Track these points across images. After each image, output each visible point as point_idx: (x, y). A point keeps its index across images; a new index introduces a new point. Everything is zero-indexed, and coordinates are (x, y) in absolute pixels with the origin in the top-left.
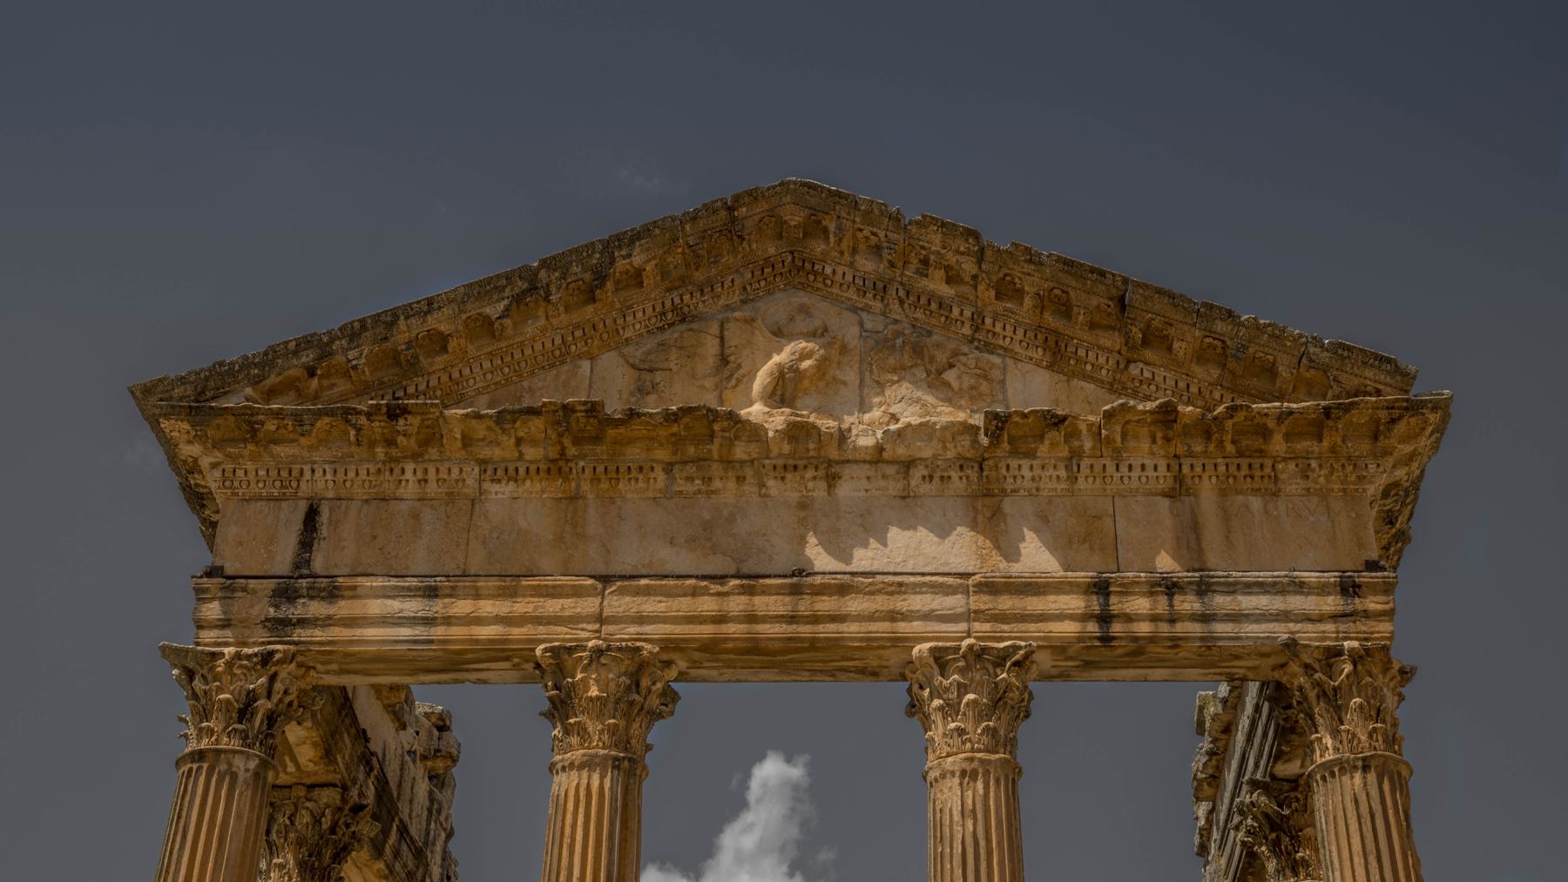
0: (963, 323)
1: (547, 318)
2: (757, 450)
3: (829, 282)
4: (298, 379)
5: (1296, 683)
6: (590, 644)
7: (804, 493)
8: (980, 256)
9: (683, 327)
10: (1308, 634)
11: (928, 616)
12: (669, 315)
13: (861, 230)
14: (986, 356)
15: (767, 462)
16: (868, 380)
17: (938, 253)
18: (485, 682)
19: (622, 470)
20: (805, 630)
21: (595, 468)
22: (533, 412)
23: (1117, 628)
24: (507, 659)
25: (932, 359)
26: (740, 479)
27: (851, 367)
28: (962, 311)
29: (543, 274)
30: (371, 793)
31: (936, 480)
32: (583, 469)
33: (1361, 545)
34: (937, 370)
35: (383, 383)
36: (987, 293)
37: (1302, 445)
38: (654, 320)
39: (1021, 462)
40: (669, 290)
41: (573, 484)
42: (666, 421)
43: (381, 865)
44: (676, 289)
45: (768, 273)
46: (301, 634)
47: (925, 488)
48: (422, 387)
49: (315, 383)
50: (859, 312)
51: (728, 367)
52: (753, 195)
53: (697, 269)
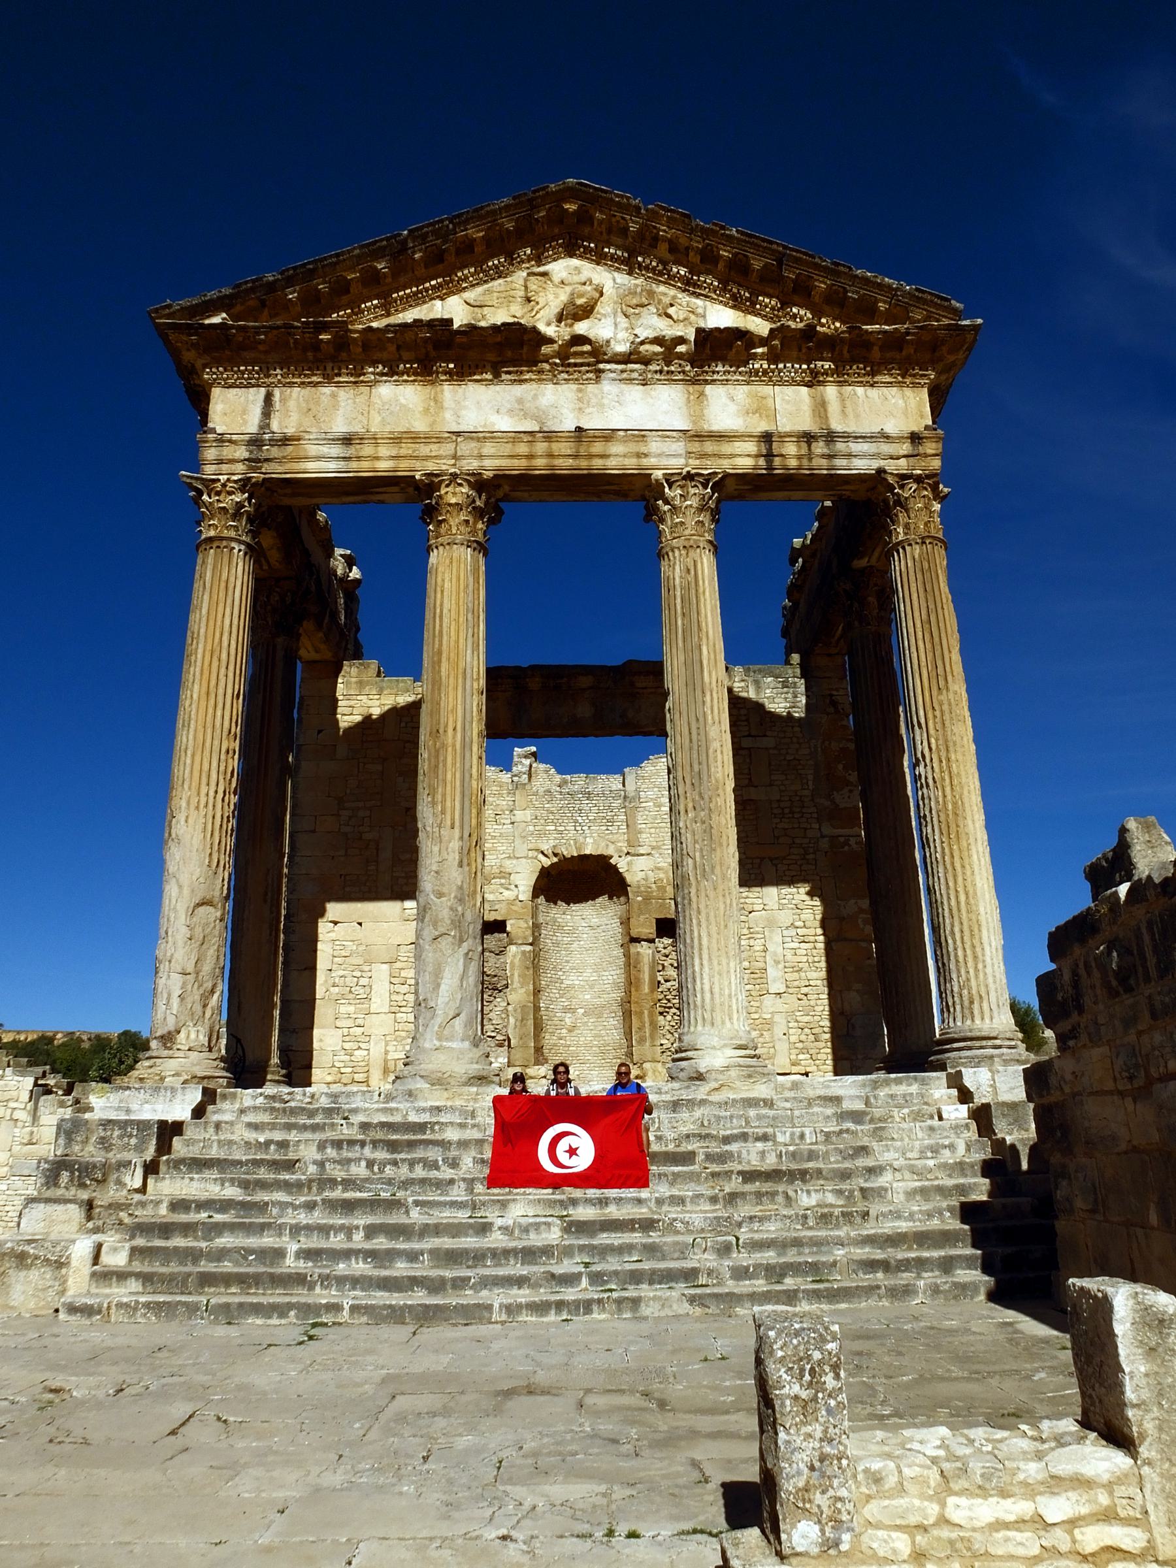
6: (452, 470)
9: (501, 281)
10: (891, 466)
11: (659, 455)
14: (694, 300)
17: (664, 231)
18: (382, 502)
20: (584, 463)
22: (405, 326)
23: (777, 461)
24: (396, 484)
25: (660, 301)
30: (313, 588)
33: (922, 417)
37: (888, 355)
43: (321, 635)
46: (266, 467)
47: (658, 376)
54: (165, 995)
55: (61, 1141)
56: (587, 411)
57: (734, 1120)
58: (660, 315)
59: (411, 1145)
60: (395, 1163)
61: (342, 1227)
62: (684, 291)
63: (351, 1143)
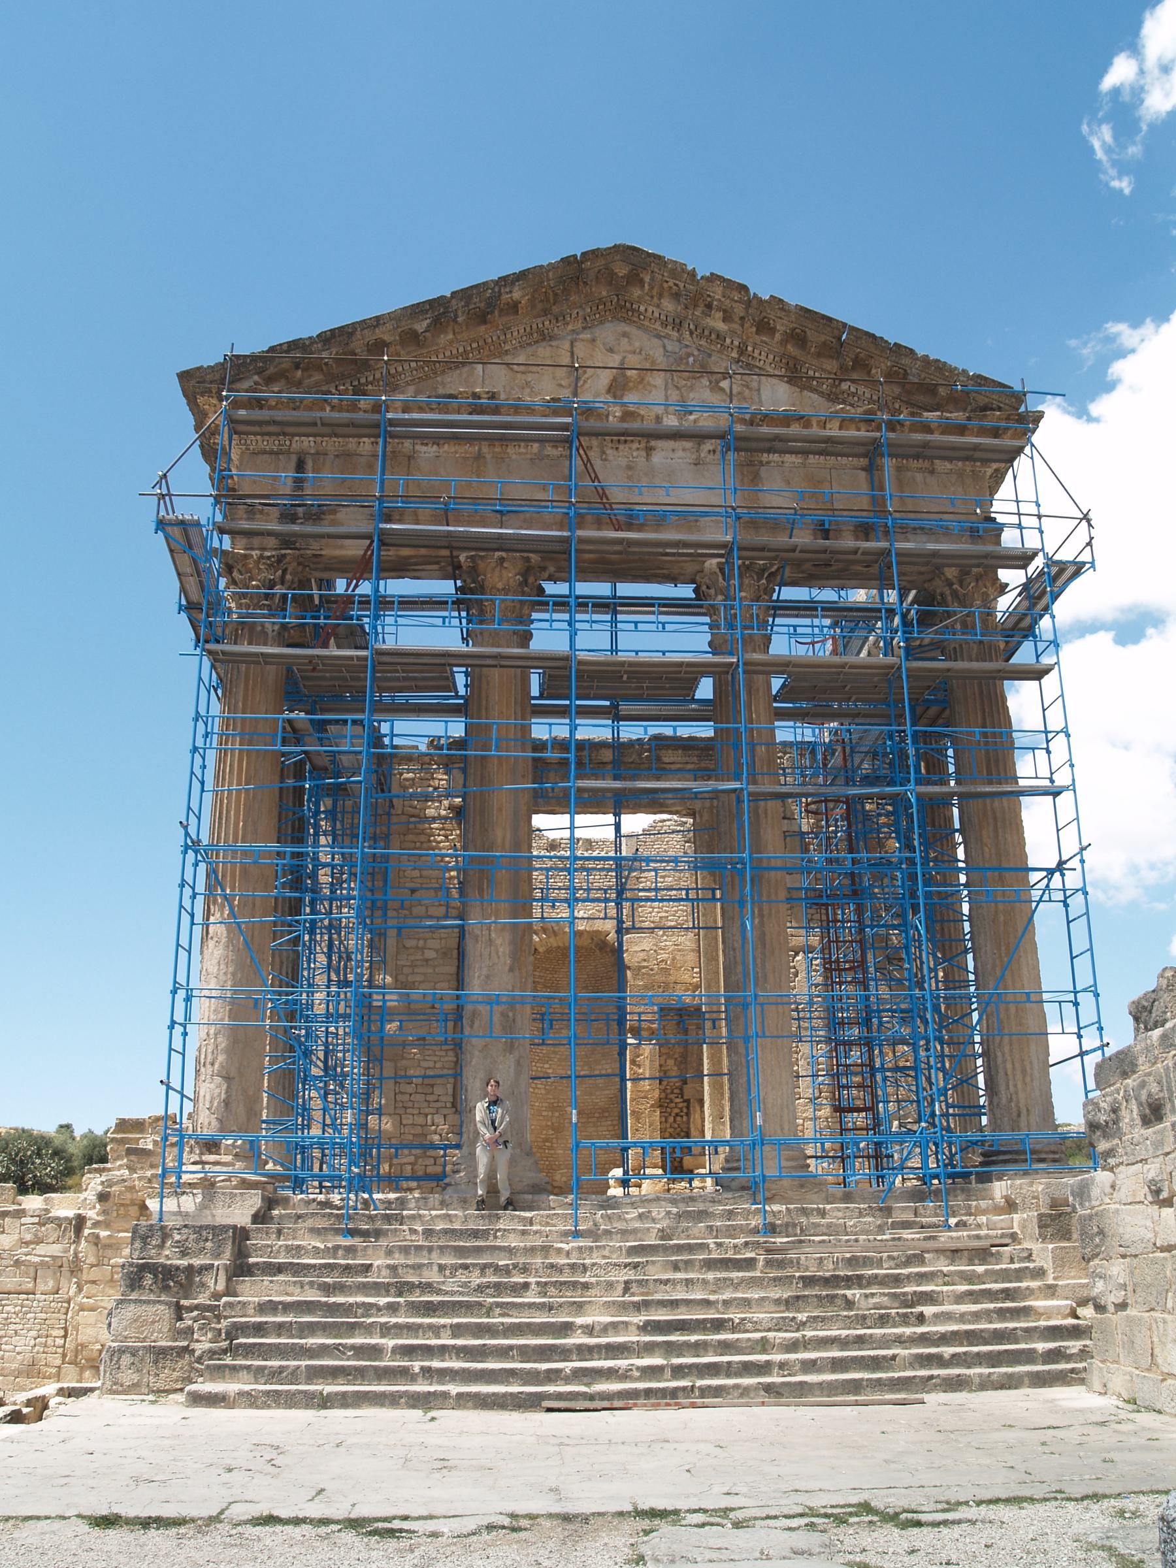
4: (287, 371)
5: (938, 591)
8: (748, 304)
9: (544, 344)
16: (670, 386)
24: (437, 563)
29: (454, 302)
35: (343, 375)
40: (535, 317)
47: (711, 456)
48: (370, 379)
49: (299, 373)
52: (594, 254)
54: (208, 1098)
55: (138, 1245)
57: (790, 1229)
58: (712, 390)
59: (478, 1250)
60: (466, 1267)
61: (431, 1327)
63: (419, 1248)
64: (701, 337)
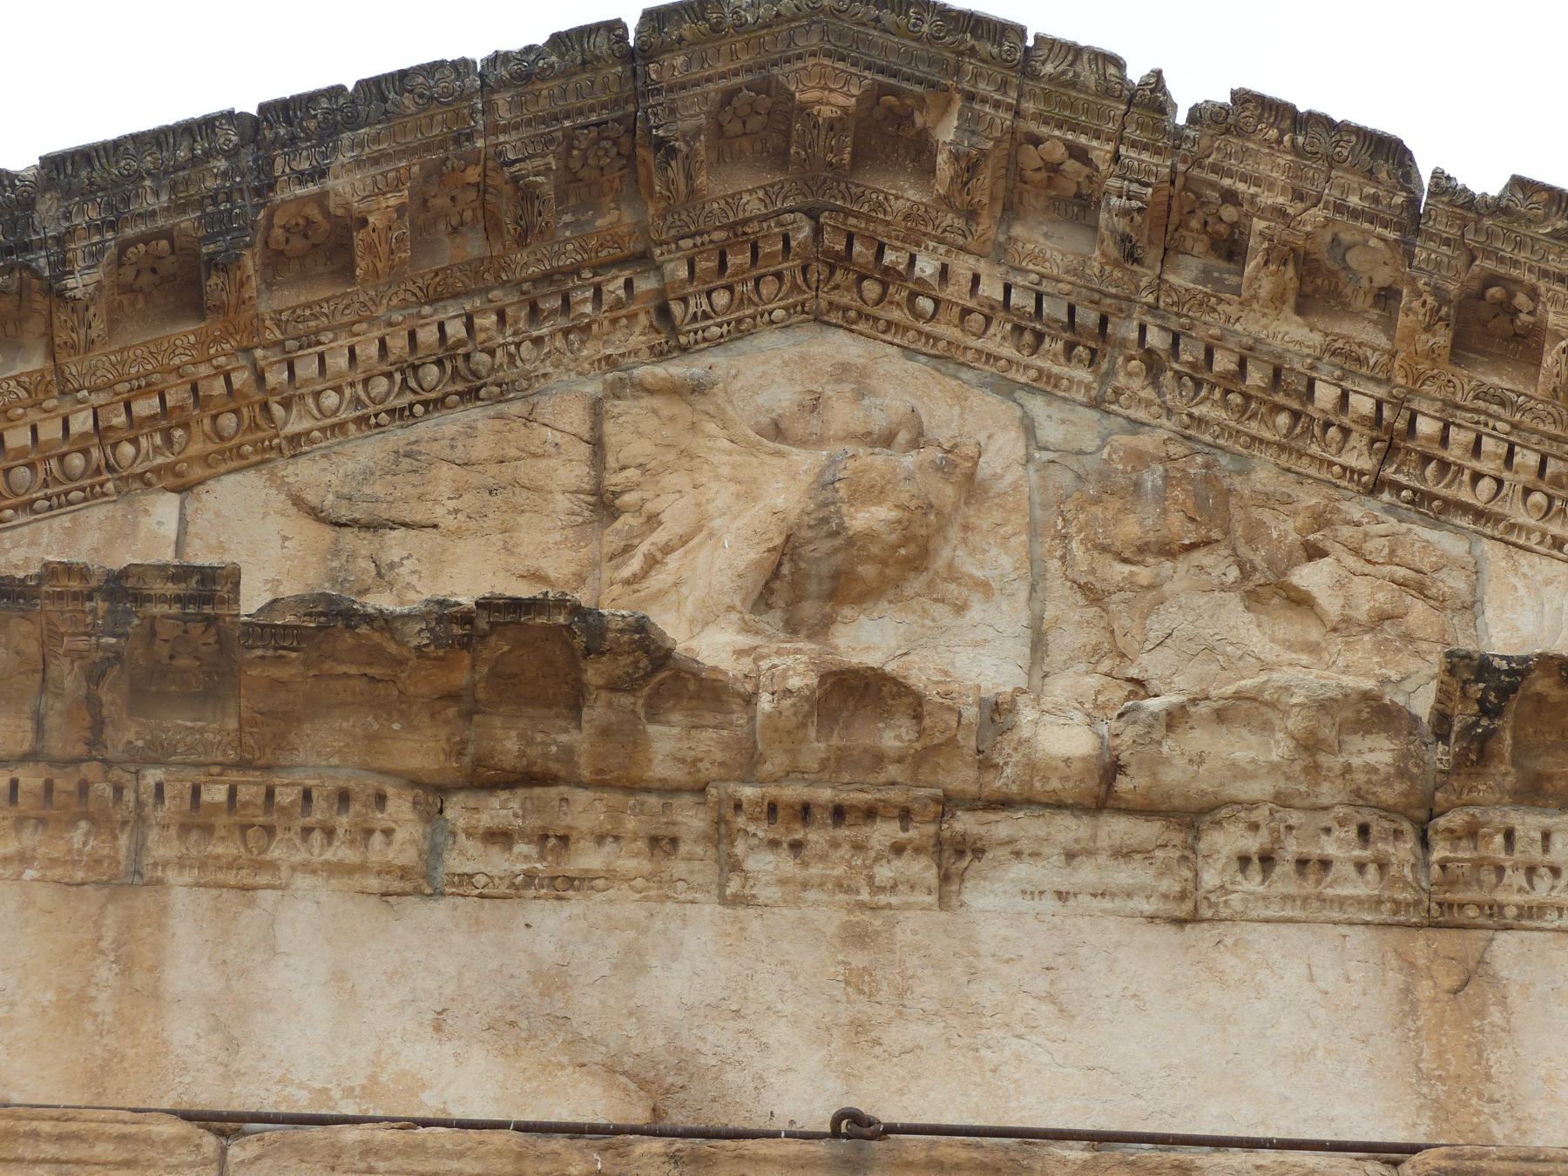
0: (1346, 432)
1: (51, 353)
2: (719, 756)
3: (925, 304)
7: (865, 896)
12: (431, 373)
13: (1036, 141)
15: (748, 792)
16: (1057, 586)
17: (1281, 212)
19: (287, 796)
21: (196, 791)
25: (1256, 531)
26: (663, 844)
27: (1006, 539)
28: (1345, 396)
29: (47, 207)
31: (1285, 868)
32: (159, 789)
34: (1271, 564)
36: (1425, 341)
38: (381, 385)
39: (1548, 821)
41: (124, 840)
42: (435, 640)
44: (456, 296)
45: (740, 270)
47: (1253, 883)
50: (1018, 394)
51: (618, 524)
53: (522, 240)
56: (894, 1037)
58: (1254, 598)
62: (1376, 486)
64: (1198, 379)
